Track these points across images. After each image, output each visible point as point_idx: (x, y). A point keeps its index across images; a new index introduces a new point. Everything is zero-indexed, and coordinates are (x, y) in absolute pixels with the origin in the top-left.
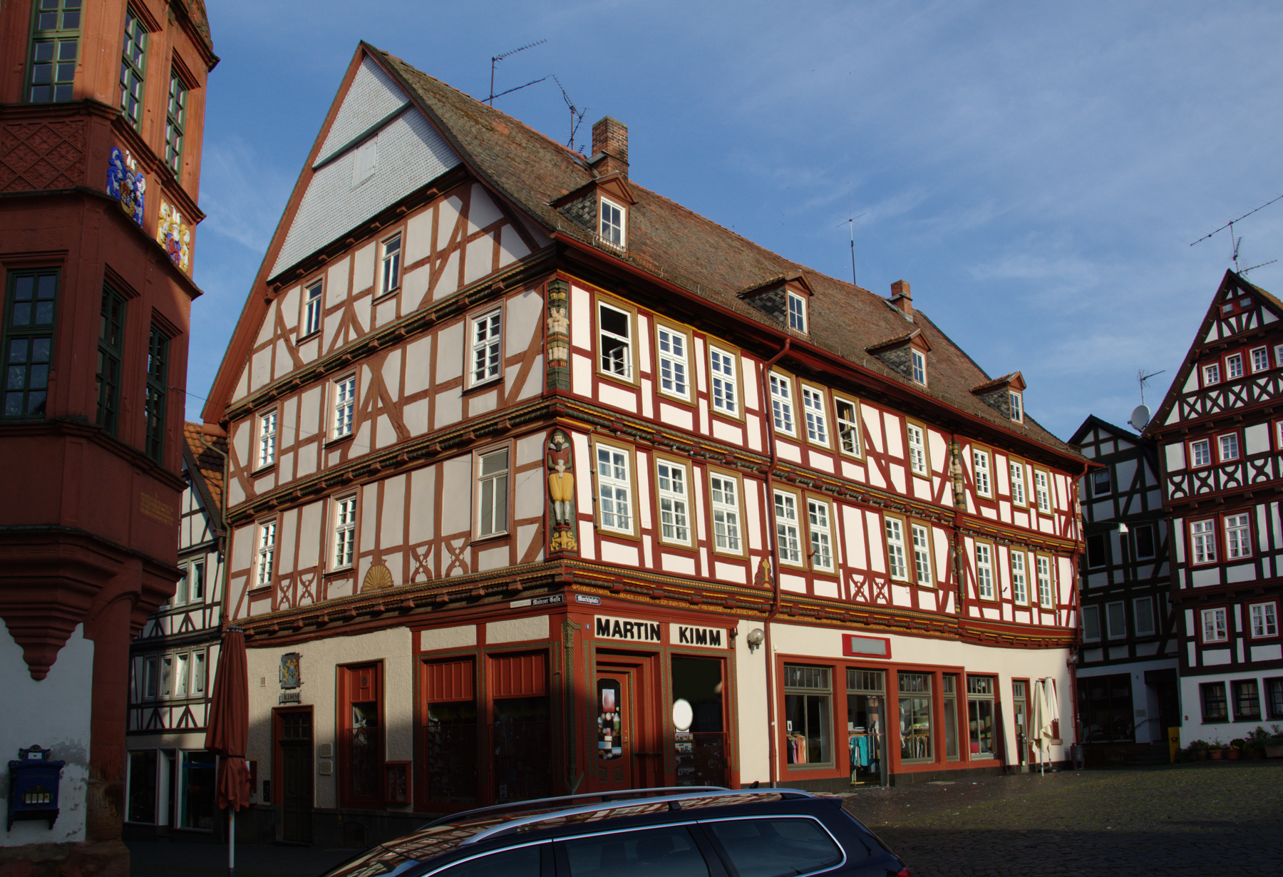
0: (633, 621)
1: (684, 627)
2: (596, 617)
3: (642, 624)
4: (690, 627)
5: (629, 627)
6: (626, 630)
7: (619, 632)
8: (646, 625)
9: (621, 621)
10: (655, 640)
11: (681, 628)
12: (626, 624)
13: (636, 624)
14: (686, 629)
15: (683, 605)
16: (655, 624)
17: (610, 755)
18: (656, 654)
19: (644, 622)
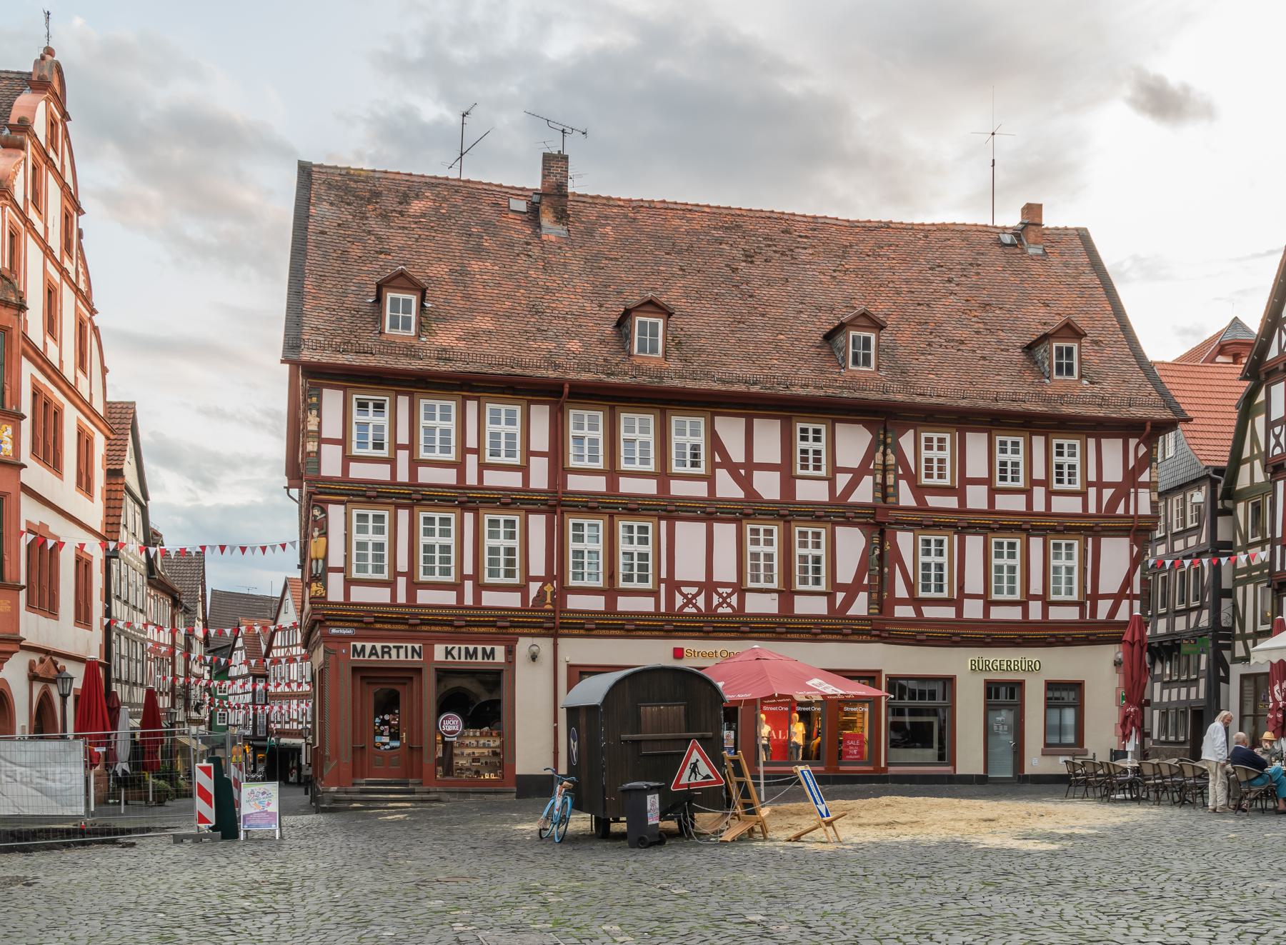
0: (391, 645)
1: (450, 647)
2: (352, 643)
3: (402, 647)
4: (457, 646)
5: (386, 650)
6: (383, 653)
7: (376, 654)
8: (406, 647)
9: (379, 646)
10: (416, 658)
11: (447, 648)
12: (383, 647)
13: (394, 647)
14: (453, 648)
15: (446, 629)
16: (417, 646)
17: (387, 747)
18: (419, 671)
19: (404, 645)
